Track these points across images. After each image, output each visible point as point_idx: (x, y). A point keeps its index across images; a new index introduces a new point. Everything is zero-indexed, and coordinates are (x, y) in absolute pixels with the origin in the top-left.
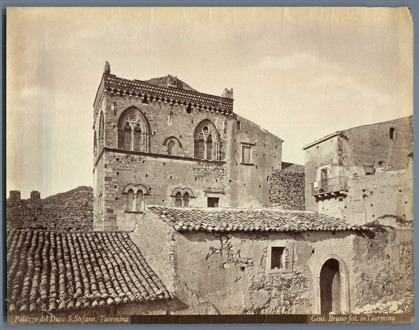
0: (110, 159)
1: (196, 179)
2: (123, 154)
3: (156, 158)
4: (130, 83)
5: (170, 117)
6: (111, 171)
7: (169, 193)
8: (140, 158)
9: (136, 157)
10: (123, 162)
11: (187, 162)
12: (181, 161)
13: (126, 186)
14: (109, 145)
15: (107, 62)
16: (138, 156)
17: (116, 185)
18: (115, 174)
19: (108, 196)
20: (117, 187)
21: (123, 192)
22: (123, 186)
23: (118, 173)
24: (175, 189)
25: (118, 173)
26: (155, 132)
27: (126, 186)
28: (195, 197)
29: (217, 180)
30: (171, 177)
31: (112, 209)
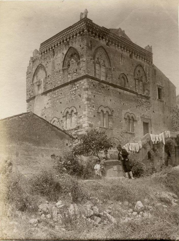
0: (90, 84)
1: (136, 107)
2: (97, 82)
3: (115, 88)
4: (100, 28)
5: (122, 59)
6: (91, 94)
7: (123, 116)
8: (107, 86)
9: (104, 85)
10: (97, 88)
11: (132, 94)
12: (128, 93)
13: (99, 107)
14: (89, 73)
15: (86, 10)
16: (106, 85)
17: (93, 105)
18: (93, 97)
19: (89, 114)
20: (94, 107)
21: (98, 111)
22: (98, 107)
23: (94, 96)
24: (126, 113)
25: (94, 96)
26: (114, 69)
27: (99, 107)
28: (136, 121)
29: (147, 110)
30: (124, 104)
31: (92, 124)
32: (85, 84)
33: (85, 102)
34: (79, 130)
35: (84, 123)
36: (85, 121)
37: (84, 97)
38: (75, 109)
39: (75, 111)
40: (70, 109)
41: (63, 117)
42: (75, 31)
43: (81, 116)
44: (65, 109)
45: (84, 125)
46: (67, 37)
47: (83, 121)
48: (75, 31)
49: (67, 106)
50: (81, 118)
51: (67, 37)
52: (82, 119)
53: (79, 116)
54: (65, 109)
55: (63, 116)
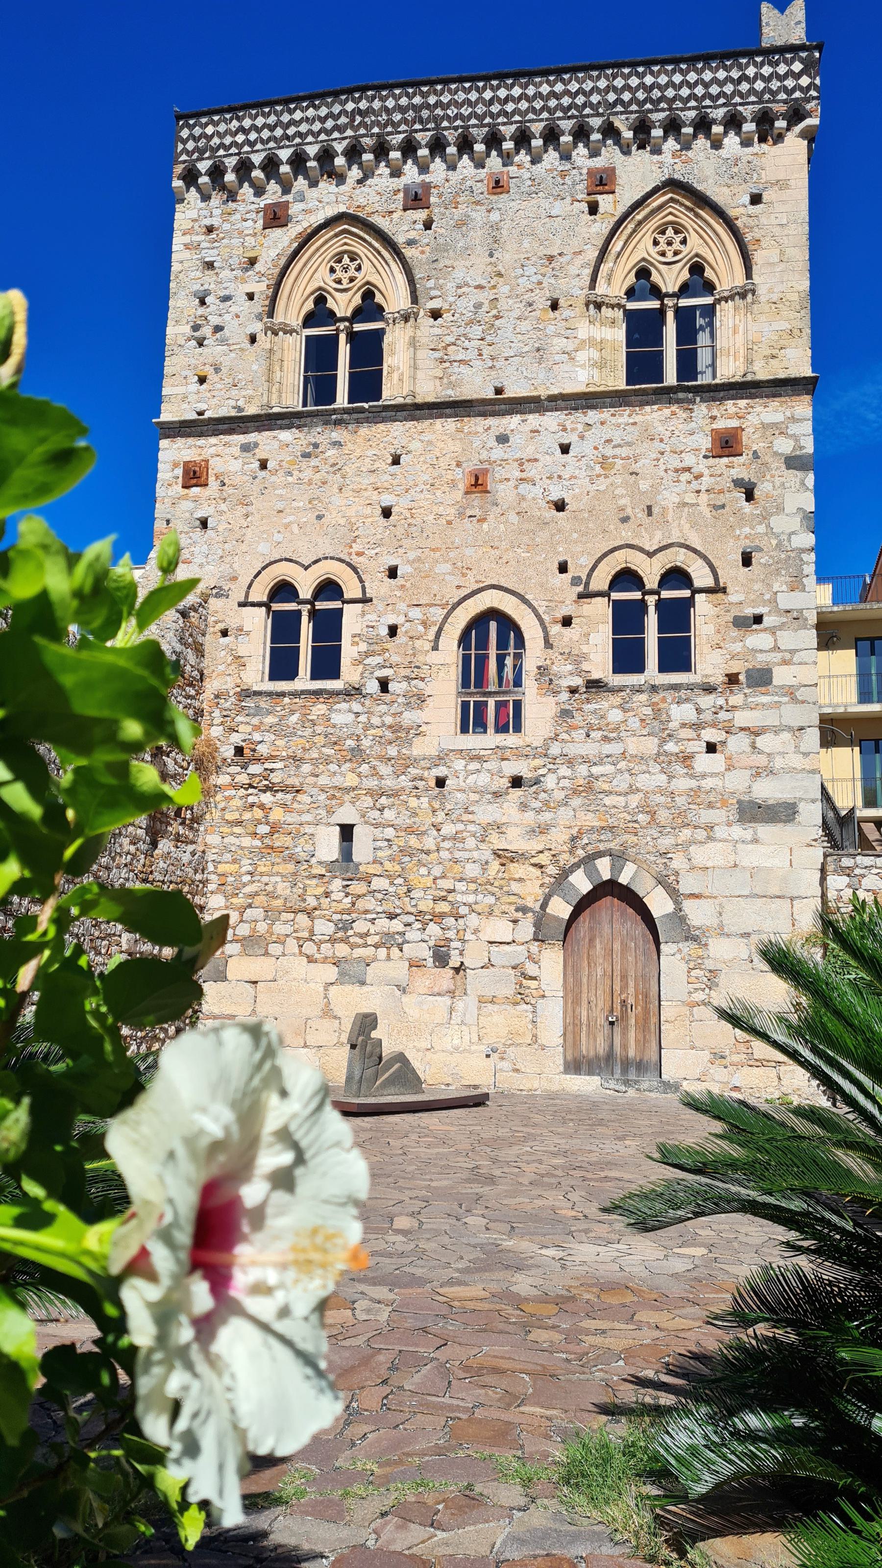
32: (793, 429)
33: (793, 533)
34: (736, 699)
35: (785, 662)
36: (793, 652)
37: (790, 506)
38: (700, 562)
39: (701, 577)
40: (650, 555)
41: (581, 596)
42: (722, 101)
43: (758, 619)
44: (605, 555)
45: (781, 676)
46: (650, 111)
47: (776, 648)
48: (722, 101)
49: (626, 535)
50: (755, 627)
51: (650, 111)
52: (762, 635)
53: (735, 612)
54: (605, 555)
55: (580, 589)
